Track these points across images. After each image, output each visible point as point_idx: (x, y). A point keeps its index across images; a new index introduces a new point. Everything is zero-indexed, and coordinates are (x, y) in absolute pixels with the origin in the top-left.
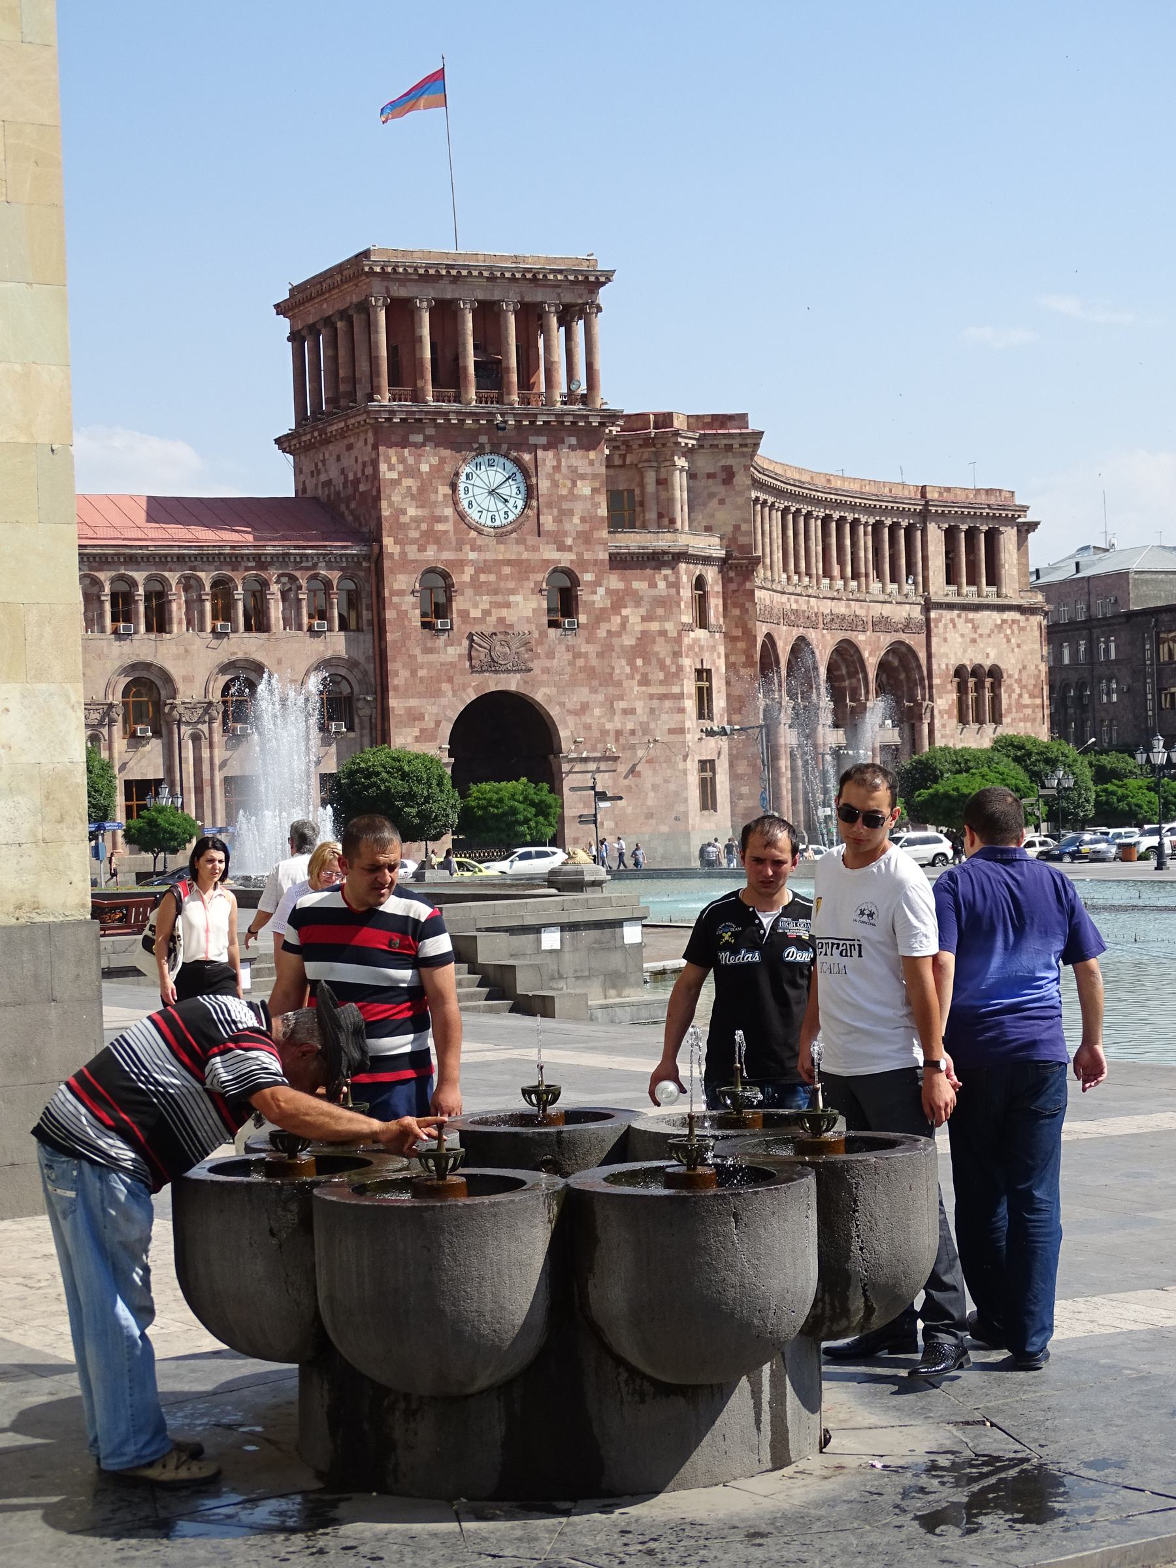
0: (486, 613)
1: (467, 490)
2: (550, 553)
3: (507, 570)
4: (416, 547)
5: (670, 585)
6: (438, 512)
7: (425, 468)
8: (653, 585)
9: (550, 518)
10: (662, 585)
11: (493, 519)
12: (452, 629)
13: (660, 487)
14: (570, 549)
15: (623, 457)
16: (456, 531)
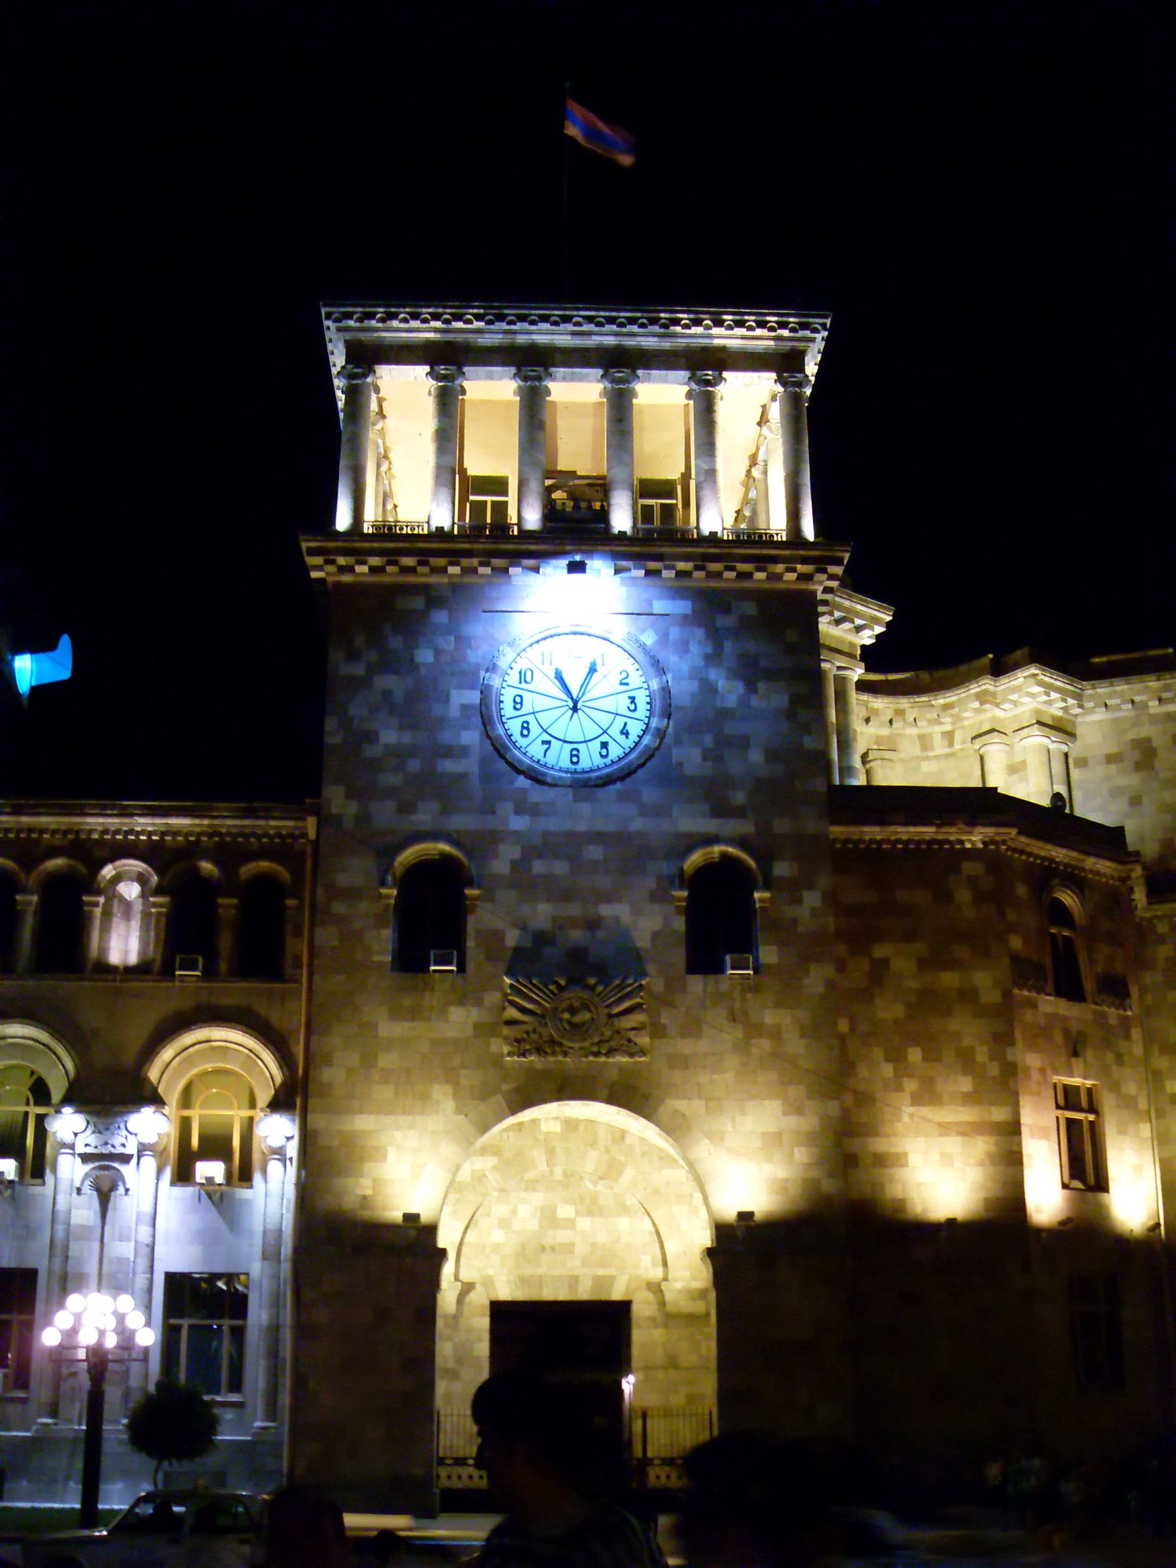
0: (541, 939)
1: (518, 703)
2: (690, 820)
3: (595, 853)
4: (390, 805)
5: (980, 898)
6: (446, 737)
7: (425, 656)
8: (944, 897)
9: (695, 754)
10: (964, 896)
11: (575, 755)
12: (462, 969)
13: (1015, 777)
14: (739, 813)
15: (949, 736)
16: (487, 777)
